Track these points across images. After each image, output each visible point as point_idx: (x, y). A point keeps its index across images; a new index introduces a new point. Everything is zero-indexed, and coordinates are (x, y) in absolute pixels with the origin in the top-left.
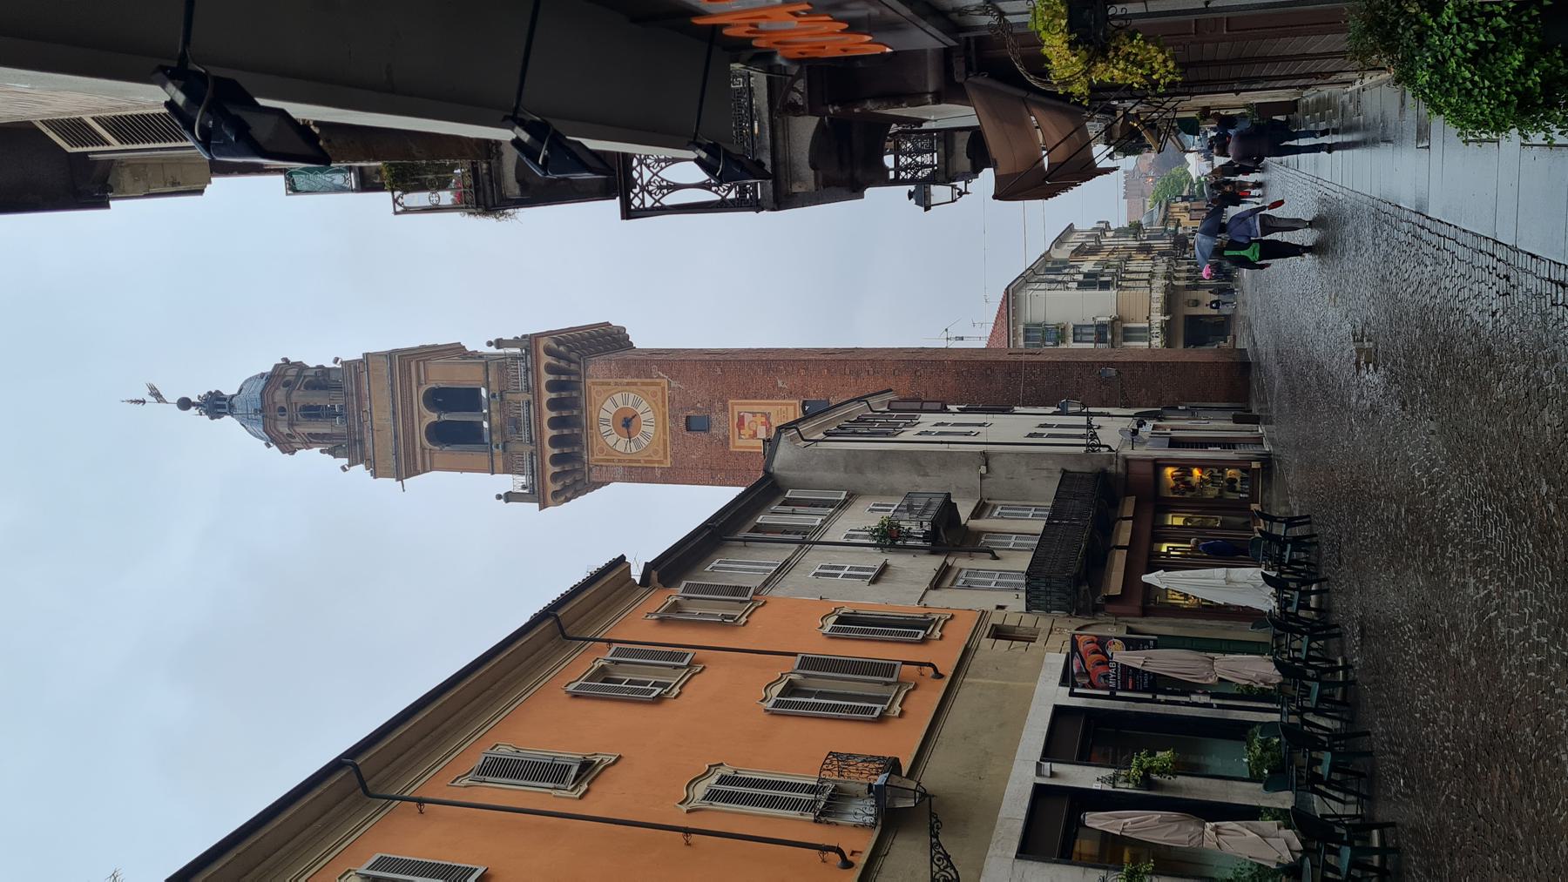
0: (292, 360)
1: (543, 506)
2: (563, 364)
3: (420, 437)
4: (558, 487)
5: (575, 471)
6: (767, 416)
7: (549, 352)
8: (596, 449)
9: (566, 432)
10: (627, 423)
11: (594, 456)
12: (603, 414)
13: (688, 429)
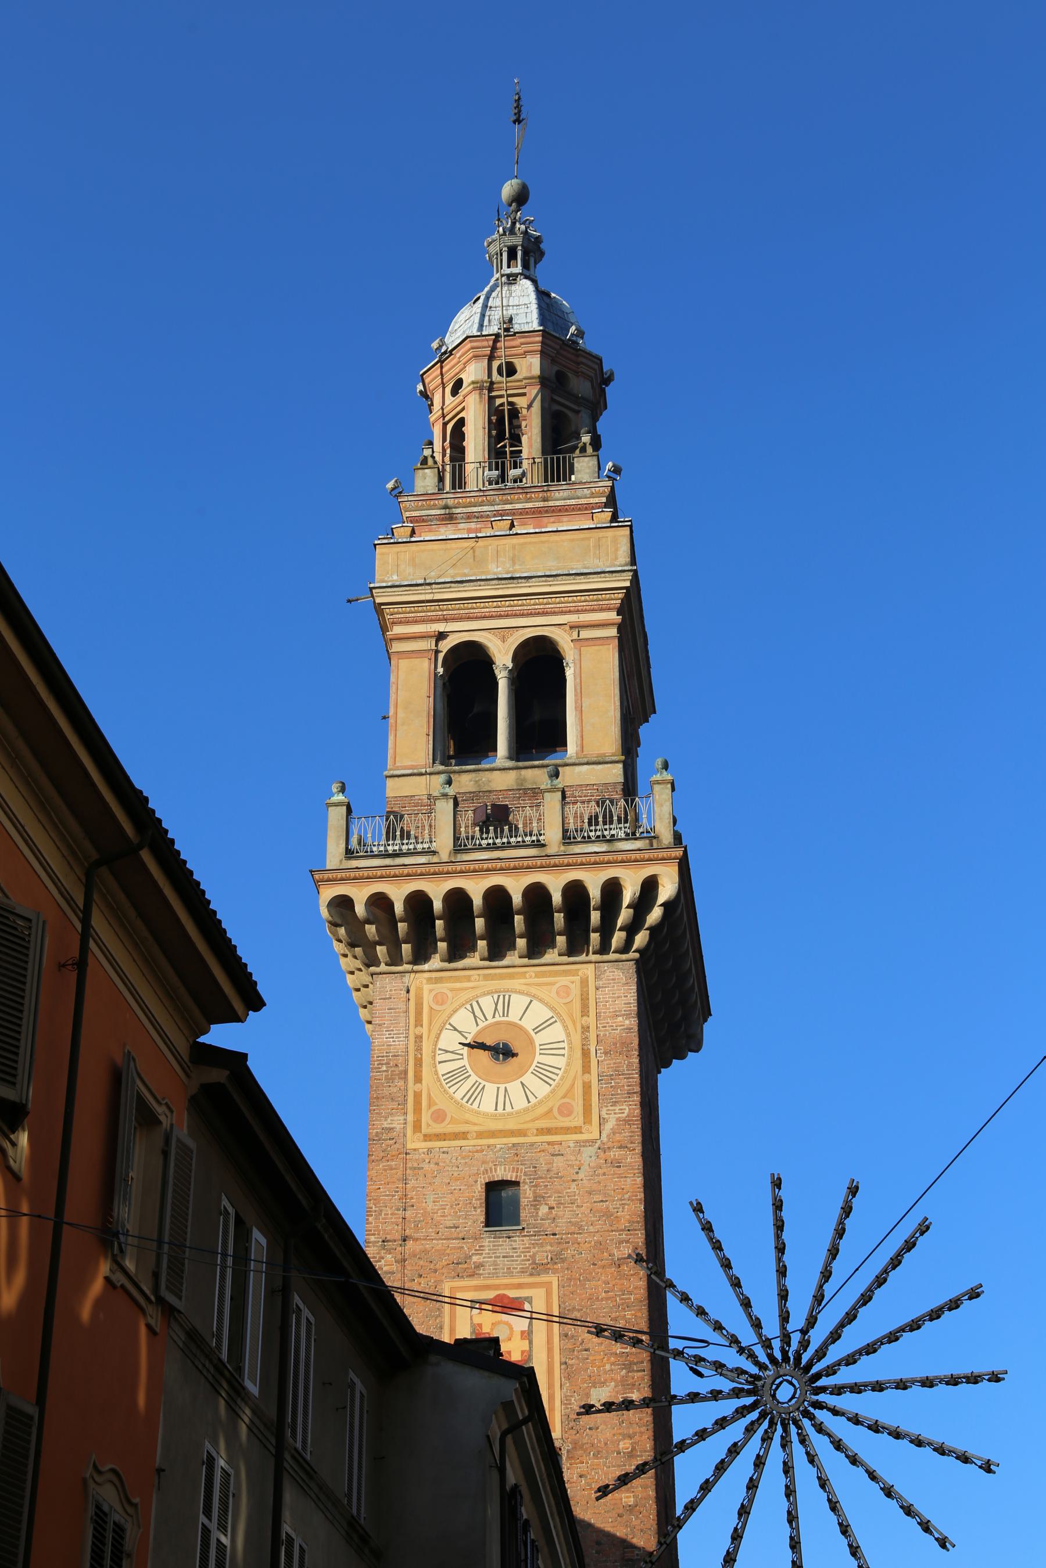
2: (625, 915)
3: (459, 632)
7: (650, 886)
8: (444, 987)
9: (480, 923)
12: (518, 1002)
13: (494, 1188)
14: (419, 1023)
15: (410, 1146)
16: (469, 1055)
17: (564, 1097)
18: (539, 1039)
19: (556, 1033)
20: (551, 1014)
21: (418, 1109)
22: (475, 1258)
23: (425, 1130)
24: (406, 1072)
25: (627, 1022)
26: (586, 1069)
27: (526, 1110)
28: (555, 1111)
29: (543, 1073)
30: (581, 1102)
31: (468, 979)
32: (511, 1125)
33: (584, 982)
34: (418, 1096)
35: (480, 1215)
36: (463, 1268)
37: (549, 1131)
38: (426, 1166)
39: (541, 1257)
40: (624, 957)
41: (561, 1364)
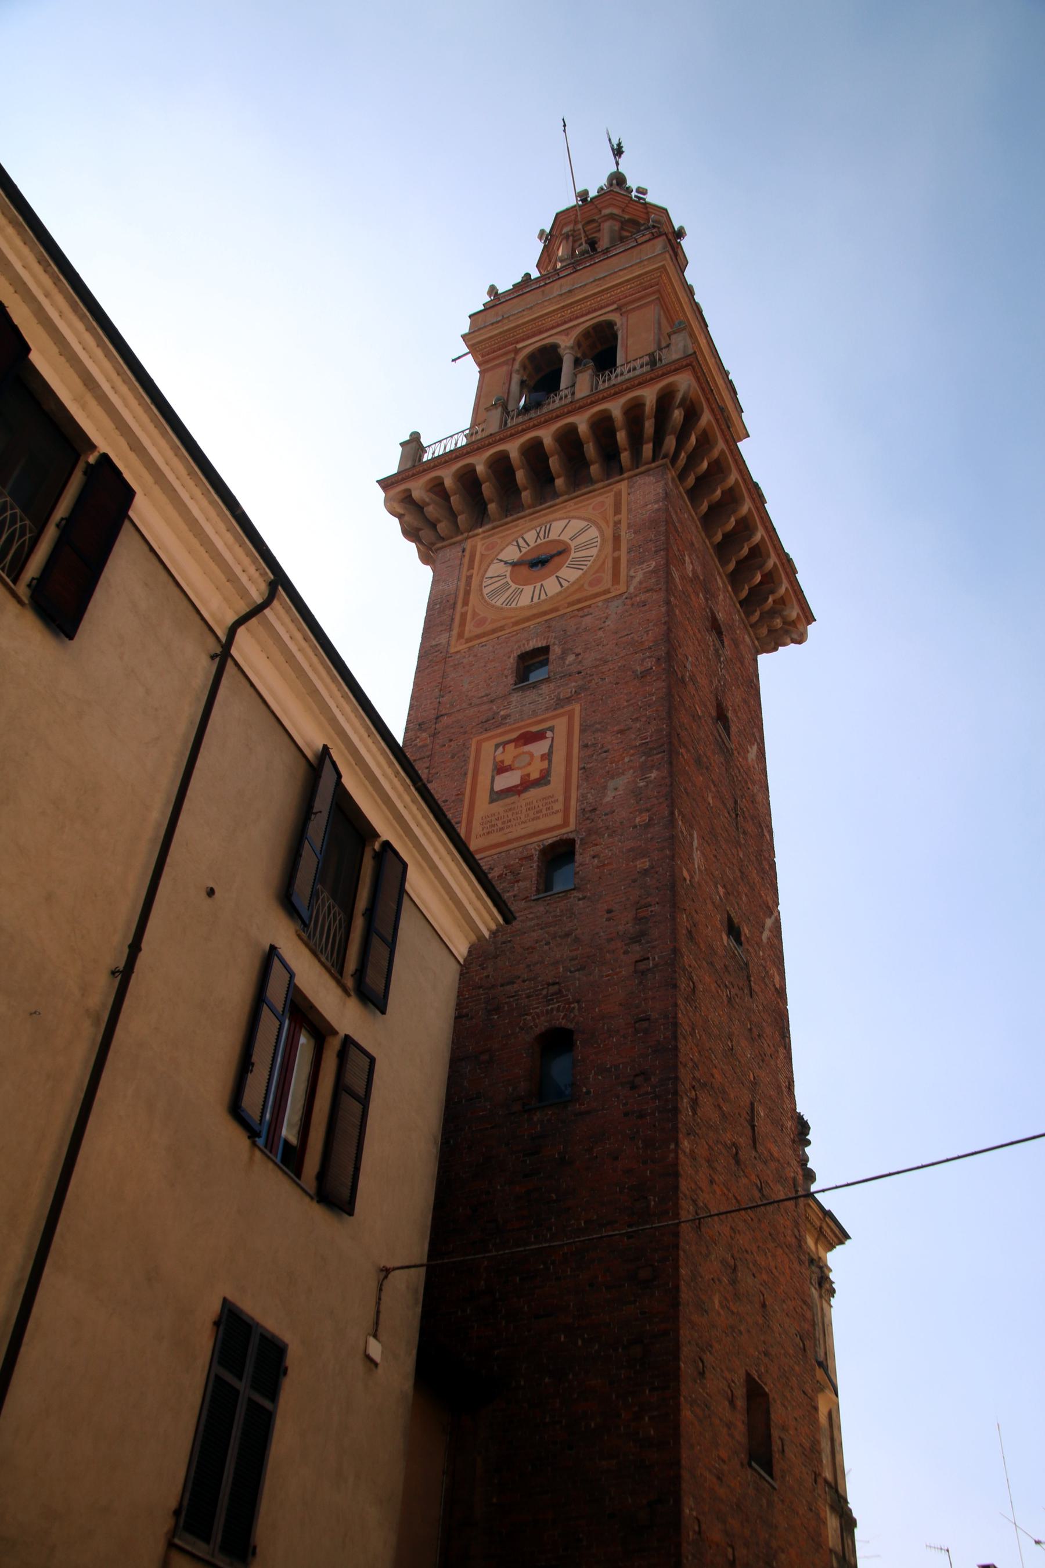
0: (684, 243)
1: (386, 484)
2: (649, 426)
4: (416, 494)
5: (453, 515)
6: (544, 779)
10: (539, 562)
11: (479, 542)
14: (471, 567)
15: (452, 650)
16: (512, 572)
17: (597, 572)
18: (573, 544)
21: (463, 623)
22: (502, 713)
23: (467, 635)
24: (455, 603)
25: (656, 506)
26: (617, 547)
27: (560, 592)
28: (586, 586)
30: (610, 571)
31: (516, 526)
32: (545, 608)
33: (618, 495)
34: (464, 616)
35: (511, 680)
36: (490, 723)
37: (579, 601)
38: (465, 661)
39: (565, 692)
40: (653, 465)
41: (580, 769)
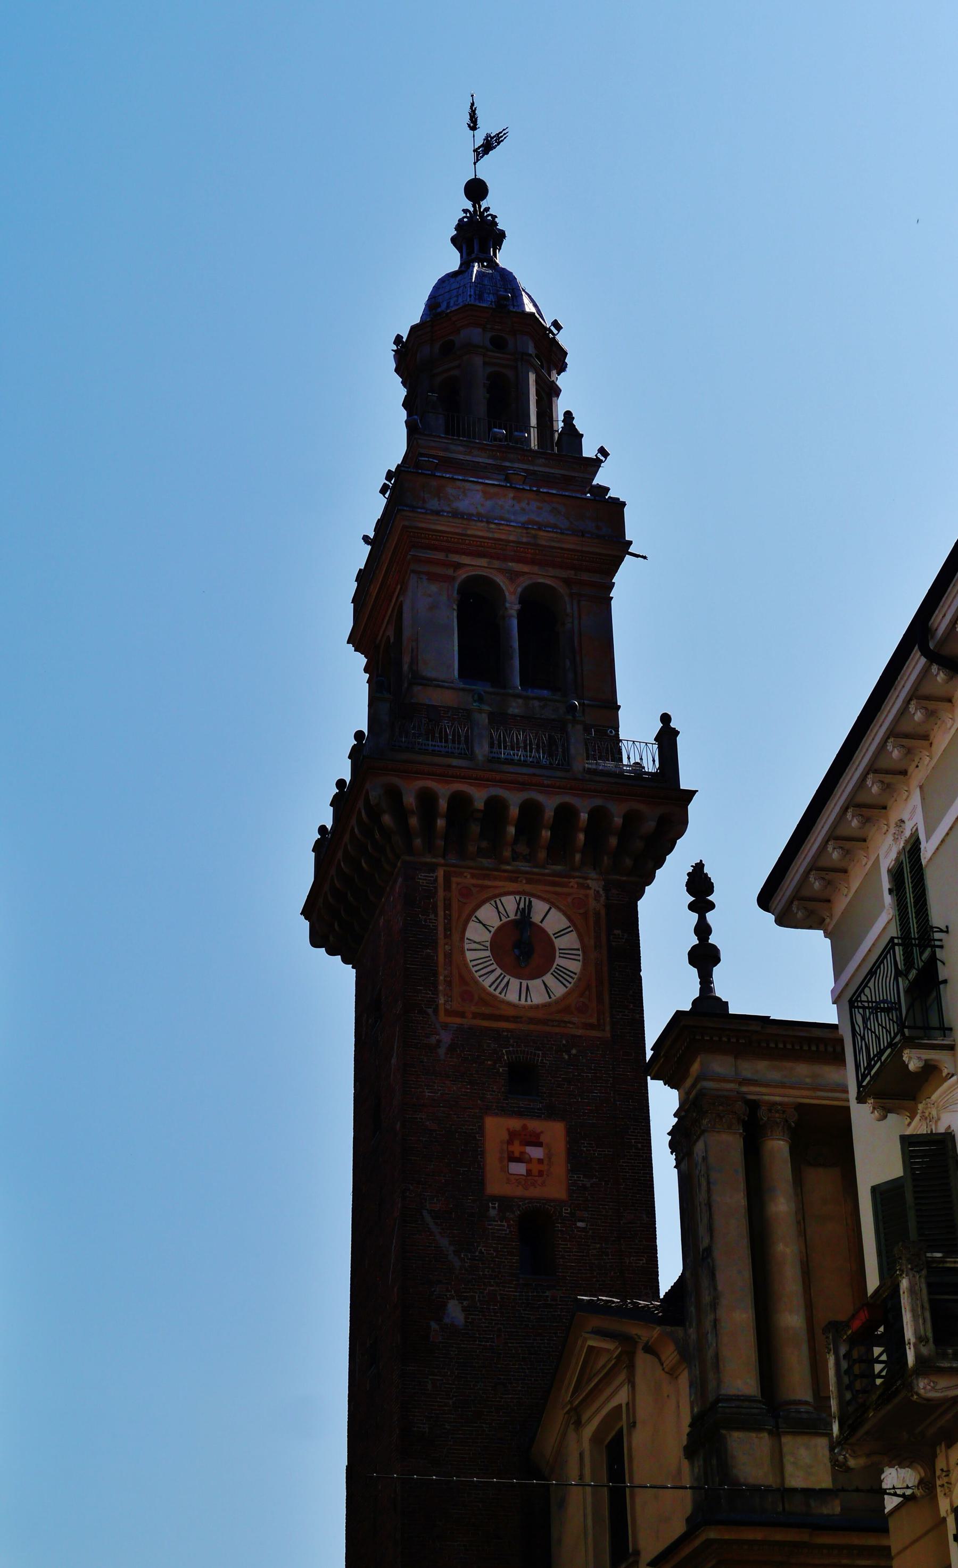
4: (410, 800)
19: (569, 941)
20: (569, 924)
29: (561, 975)
